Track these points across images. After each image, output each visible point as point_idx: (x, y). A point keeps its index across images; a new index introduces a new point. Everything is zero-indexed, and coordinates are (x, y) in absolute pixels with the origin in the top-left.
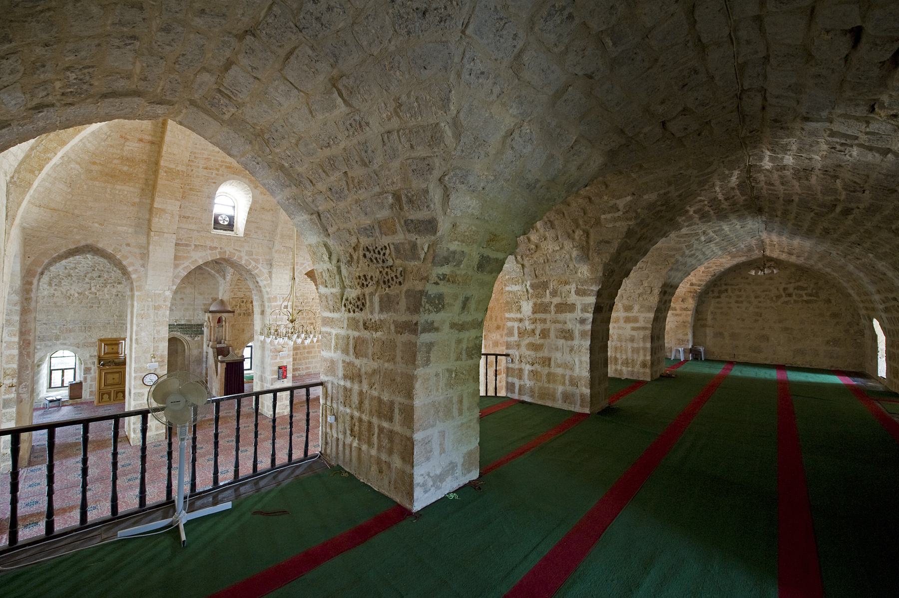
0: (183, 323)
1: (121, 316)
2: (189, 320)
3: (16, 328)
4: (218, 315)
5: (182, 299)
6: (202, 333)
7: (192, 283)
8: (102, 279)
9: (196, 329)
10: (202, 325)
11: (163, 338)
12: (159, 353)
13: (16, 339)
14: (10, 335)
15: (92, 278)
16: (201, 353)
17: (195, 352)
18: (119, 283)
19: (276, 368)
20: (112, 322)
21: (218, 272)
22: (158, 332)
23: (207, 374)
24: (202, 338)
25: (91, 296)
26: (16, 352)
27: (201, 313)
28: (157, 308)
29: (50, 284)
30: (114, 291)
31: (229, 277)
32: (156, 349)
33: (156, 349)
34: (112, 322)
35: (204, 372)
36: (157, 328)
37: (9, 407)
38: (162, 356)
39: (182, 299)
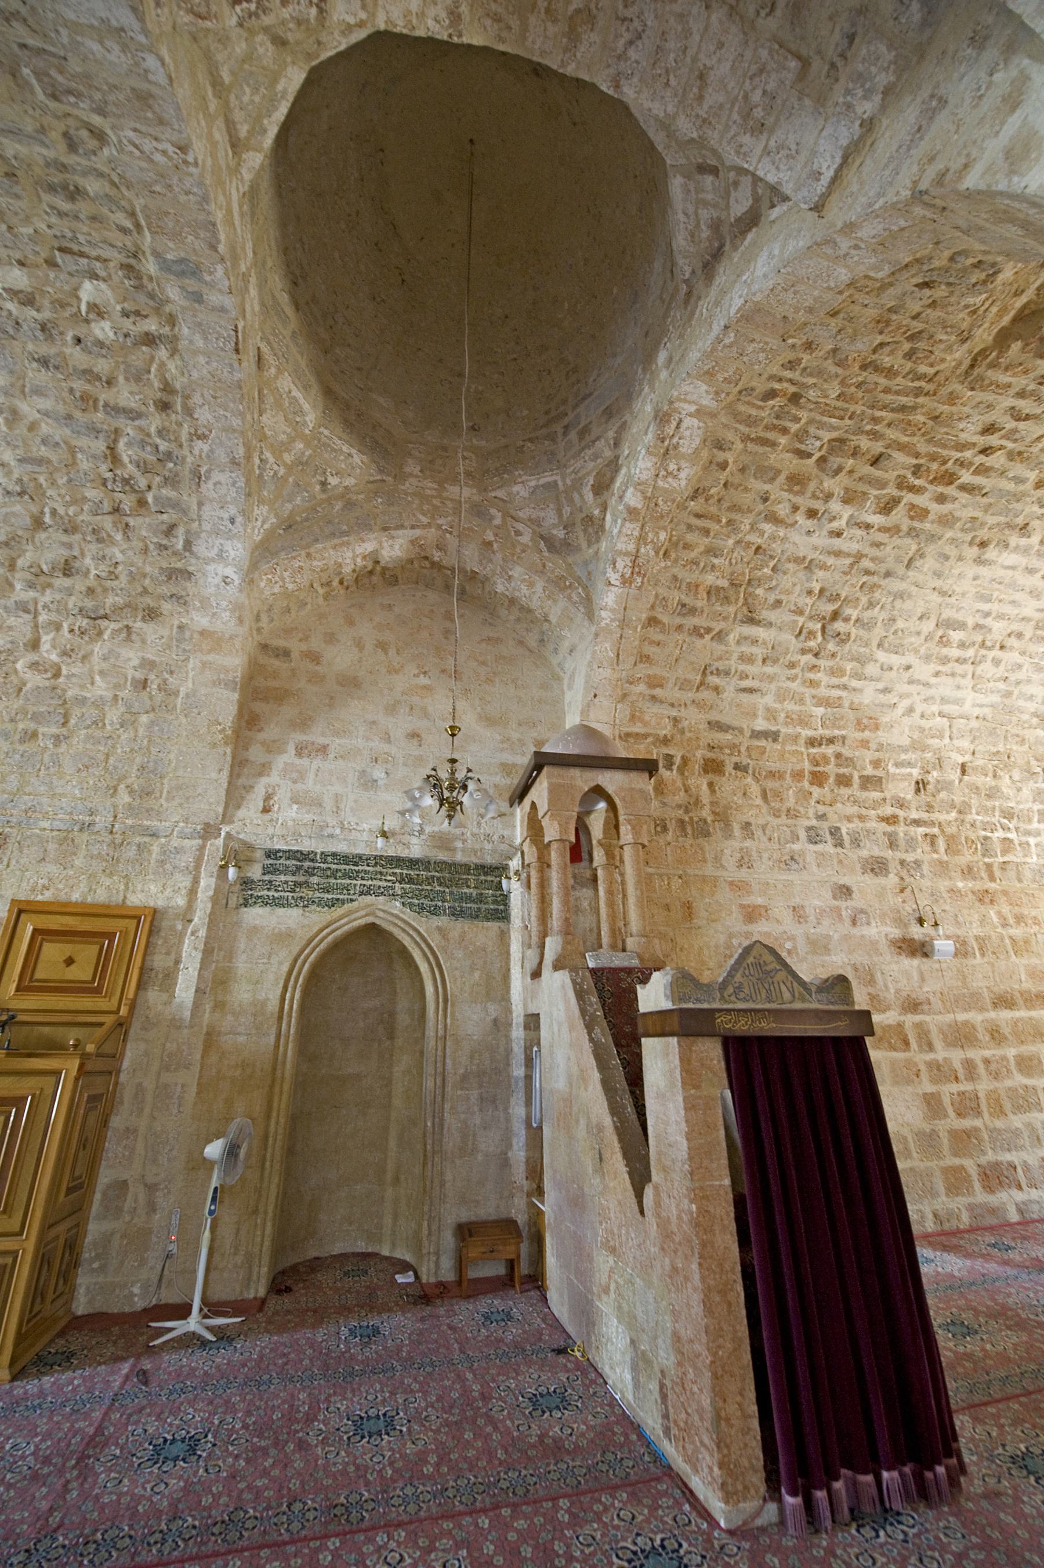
0: (416, 849)
1: (147, 793)
4: (583, 780)
5: (414, 735)
6: (501, 914)
7: (457, 675)
8: (79, 584)
9: (470, 889)
10: (500, 870)
15: (38, 578)
16: (500, 1025)
17: (471, 1019)
18: (152, 615)
20: (102, 821)
21: (559, 584)
23: (535, 1172)
24: (504, 937)
25: (35, 680)
30: (131, 656)
31: (609, 599)
34: (102, 821)
35: (519, 1153)
39: (414, 735)
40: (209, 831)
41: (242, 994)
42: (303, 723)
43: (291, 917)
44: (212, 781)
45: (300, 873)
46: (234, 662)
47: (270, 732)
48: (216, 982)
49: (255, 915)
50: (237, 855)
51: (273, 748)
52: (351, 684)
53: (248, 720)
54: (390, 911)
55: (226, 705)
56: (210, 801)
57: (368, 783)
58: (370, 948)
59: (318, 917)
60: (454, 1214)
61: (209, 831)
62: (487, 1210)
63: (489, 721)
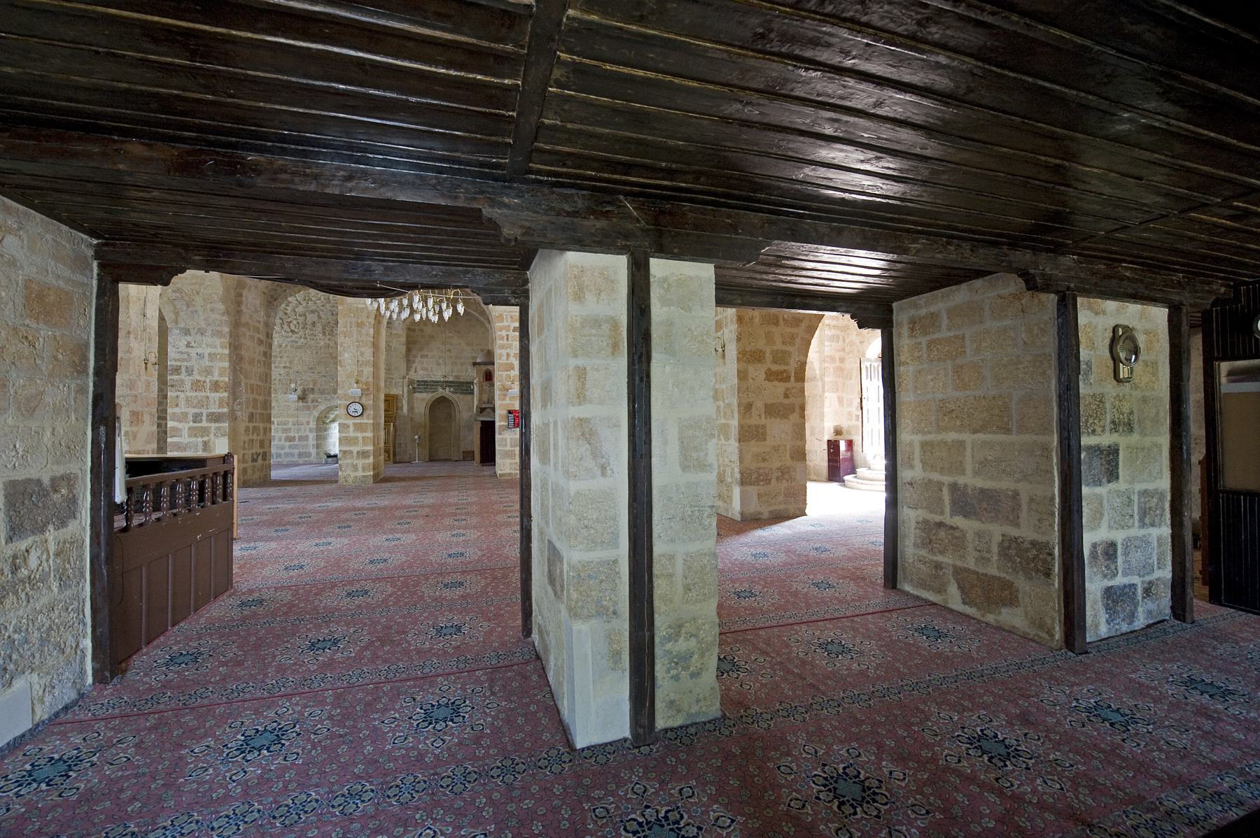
2: (457, 377)
3: (226, 340)
6: (472, 393)
9: (464, 387)
11: (368, 362)
12: (363, 379)
13: (227, 351)
14: (222, 347)
19: (505, 412)
22: (362, 354)
26: (226, 364)
27: (470, 368)
28: (360, 325)
29: (324, 334)
32: (360, 373)
33: (360, 373)
36: (363, 349)
37: (223, 422)
38: (367, 383)
40: (404, 378)
41: (416, 411)
42: (422, 349)
43: (424, 395)
44: (403, 366)
45: (426, 385)
46: (403, 339)
47: (414, 352)
48: (411, 409)
49: (417, 395)
50: (411, 382)
51: (415, 356)
52: (432, 337)
53: (409, 350)
54: (447, 392)
55: (403, 349)
56: (403, 372)
57: (439, 364)
58: (442, 400)
59: (430, 395)
60: (462, 449)
61: (404, 378)
62: (470, 449)
63: (468, 344)
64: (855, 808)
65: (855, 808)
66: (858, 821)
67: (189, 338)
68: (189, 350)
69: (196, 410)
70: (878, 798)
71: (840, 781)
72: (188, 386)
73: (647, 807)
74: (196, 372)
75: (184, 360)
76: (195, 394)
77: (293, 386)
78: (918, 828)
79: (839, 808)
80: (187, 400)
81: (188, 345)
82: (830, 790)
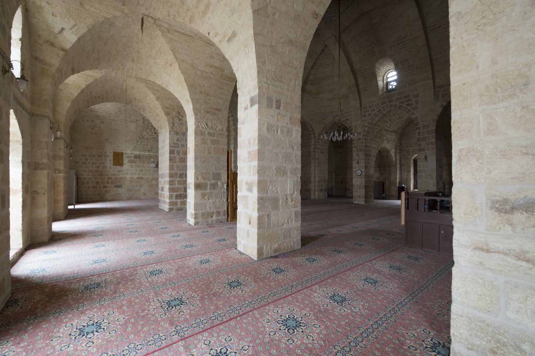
64: (294, 330)
65: (294, 330)
66: (295, 335)
67: (178, 136)
68: (178, 142)
69: (181, 172)
70: (301, 324)
71: (288, 321)
72: (178, 160)
73: (211, 349)
74: (181, 153)
75: (176, 147)
76: (180, 164)
77: (152, 160)
78: (316, 333)
79: (288, 331)
80: (177, 167)
81: (178, 140)
82: (284, 325)
